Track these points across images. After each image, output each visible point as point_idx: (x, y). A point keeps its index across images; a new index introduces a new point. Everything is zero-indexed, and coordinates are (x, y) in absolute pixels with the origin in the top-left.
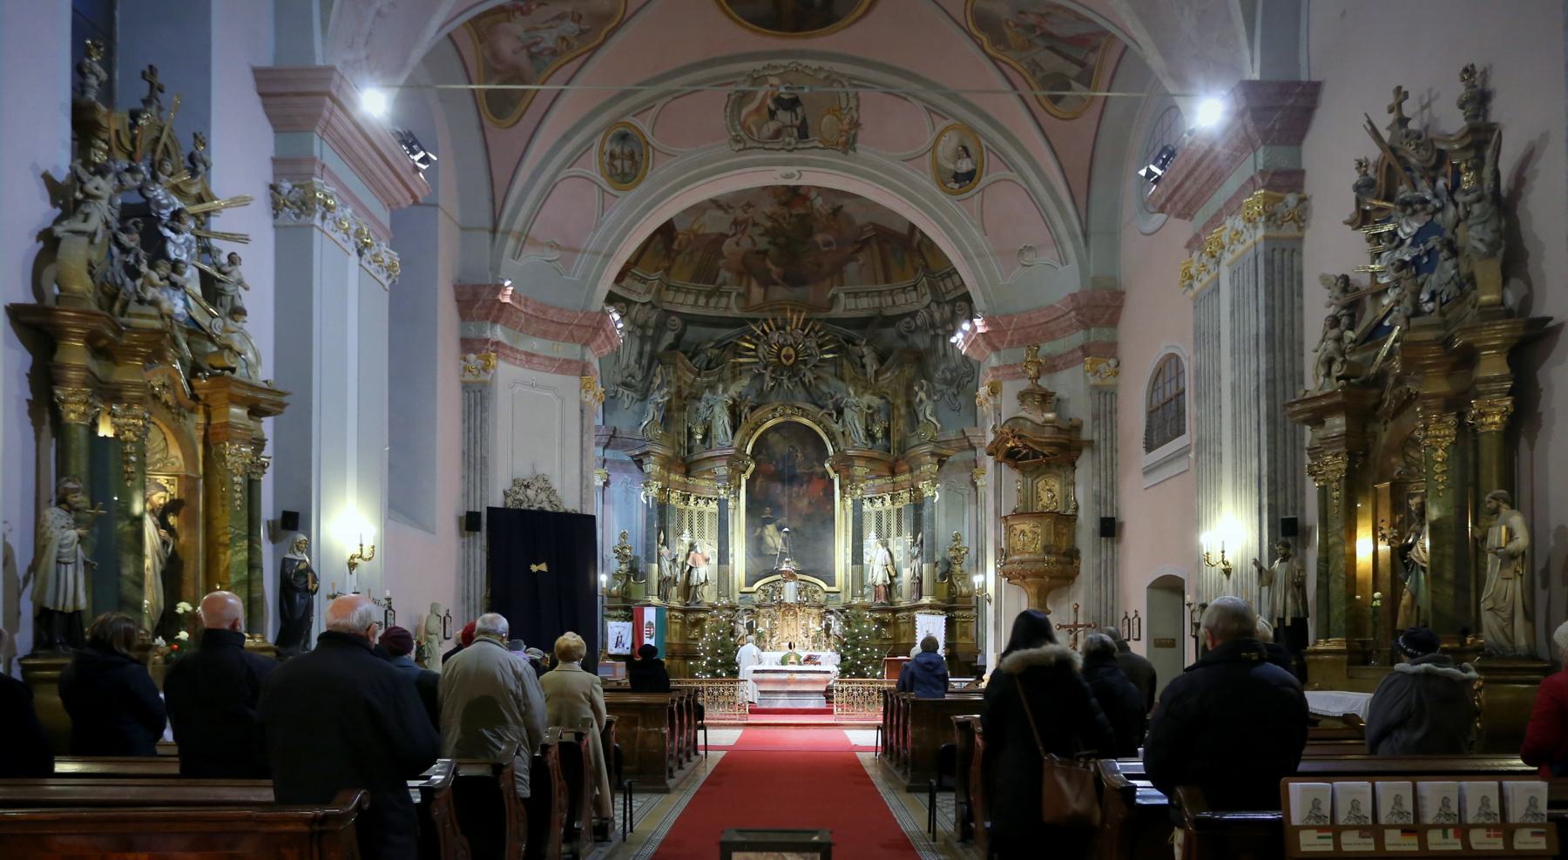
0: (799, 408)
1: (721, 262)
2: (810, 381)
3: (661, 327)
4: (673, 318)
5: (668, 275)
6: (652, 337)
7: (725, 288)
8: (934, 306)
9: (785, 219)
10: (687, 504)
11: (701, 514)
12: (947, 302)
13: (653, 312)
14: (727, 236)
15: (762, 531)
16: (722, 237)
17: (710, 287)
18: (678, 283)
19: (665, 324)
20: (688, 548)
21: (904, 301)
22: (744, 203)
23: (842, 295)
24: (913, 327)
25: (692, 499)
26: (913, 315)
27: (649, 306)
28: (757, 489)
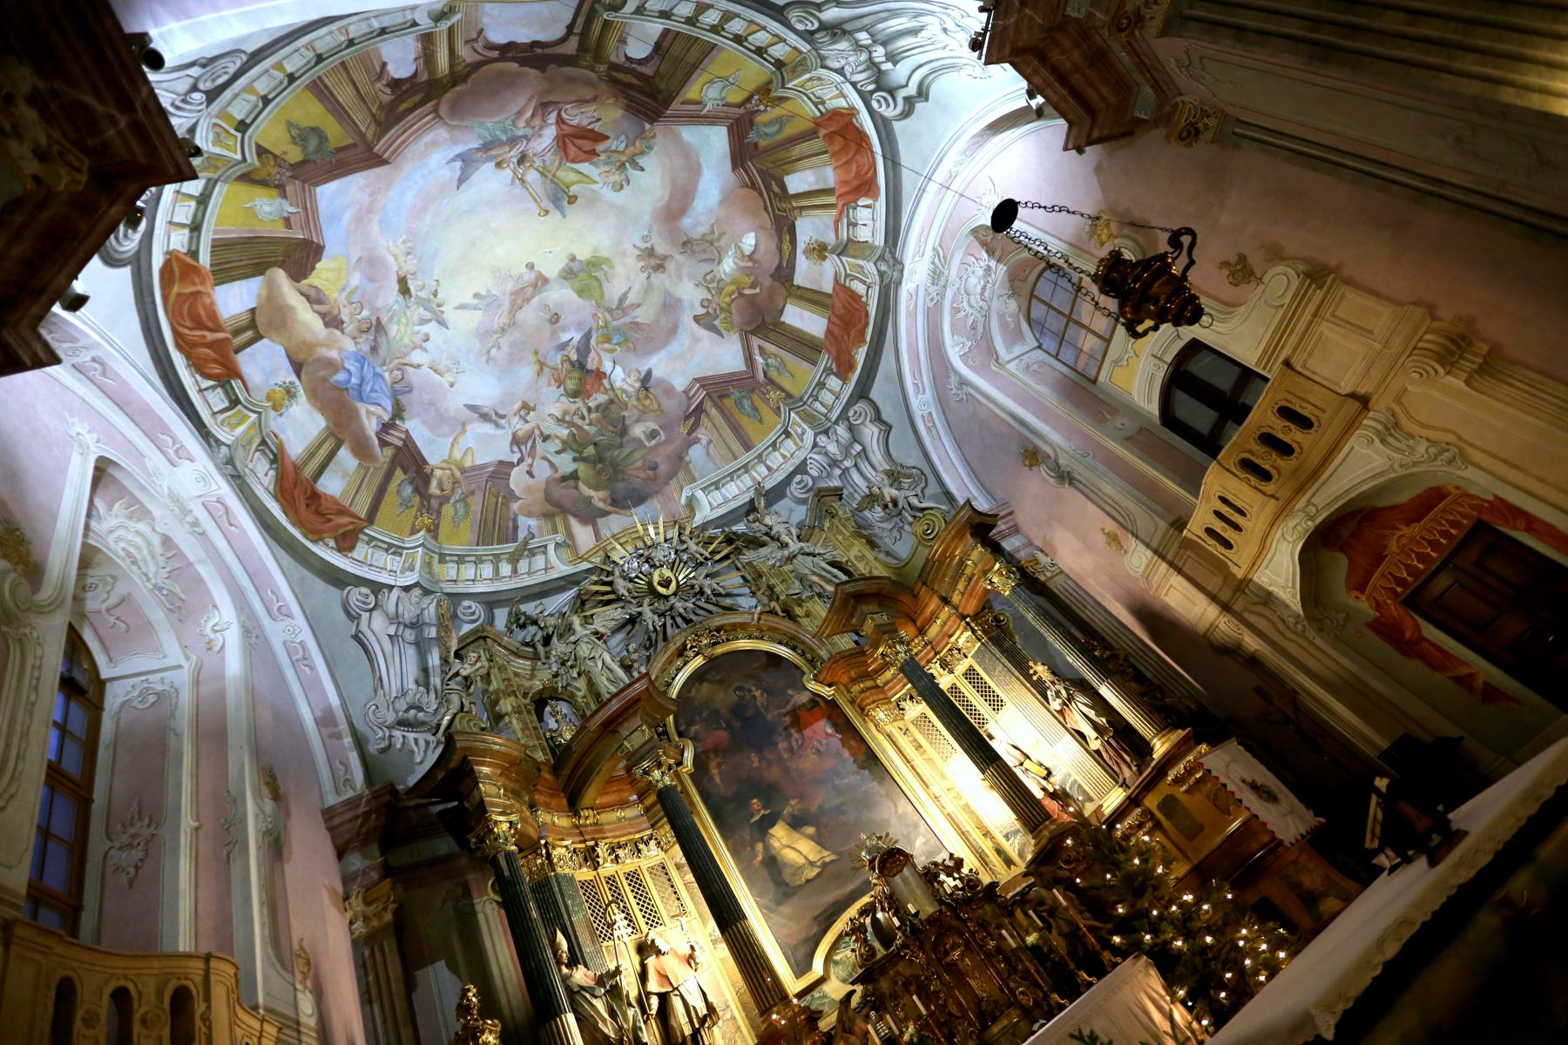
0: (718, 630)
1: (515, 506)
3: (448, 620)
4: (466, 603)
5: (436, 538)
6: (438, 639)
7: (534, 543)
8: (822, 440)
9: (583, 418)
10: (596, 866)
11: (634, 878)
12: (836, 422)
13: (427, 600)
14: (511, 465)
15: (767, 847)
16: (504, 468)
17: (510, 547)
18: (458, 548)
19: (454, 616)
21: (782, 461)
22: (518, 405)
23: (699, 494)
24: (810, 483)
25: (602, 850)
26: (801, 468)
27: (417, 592)
28: (717, 779)
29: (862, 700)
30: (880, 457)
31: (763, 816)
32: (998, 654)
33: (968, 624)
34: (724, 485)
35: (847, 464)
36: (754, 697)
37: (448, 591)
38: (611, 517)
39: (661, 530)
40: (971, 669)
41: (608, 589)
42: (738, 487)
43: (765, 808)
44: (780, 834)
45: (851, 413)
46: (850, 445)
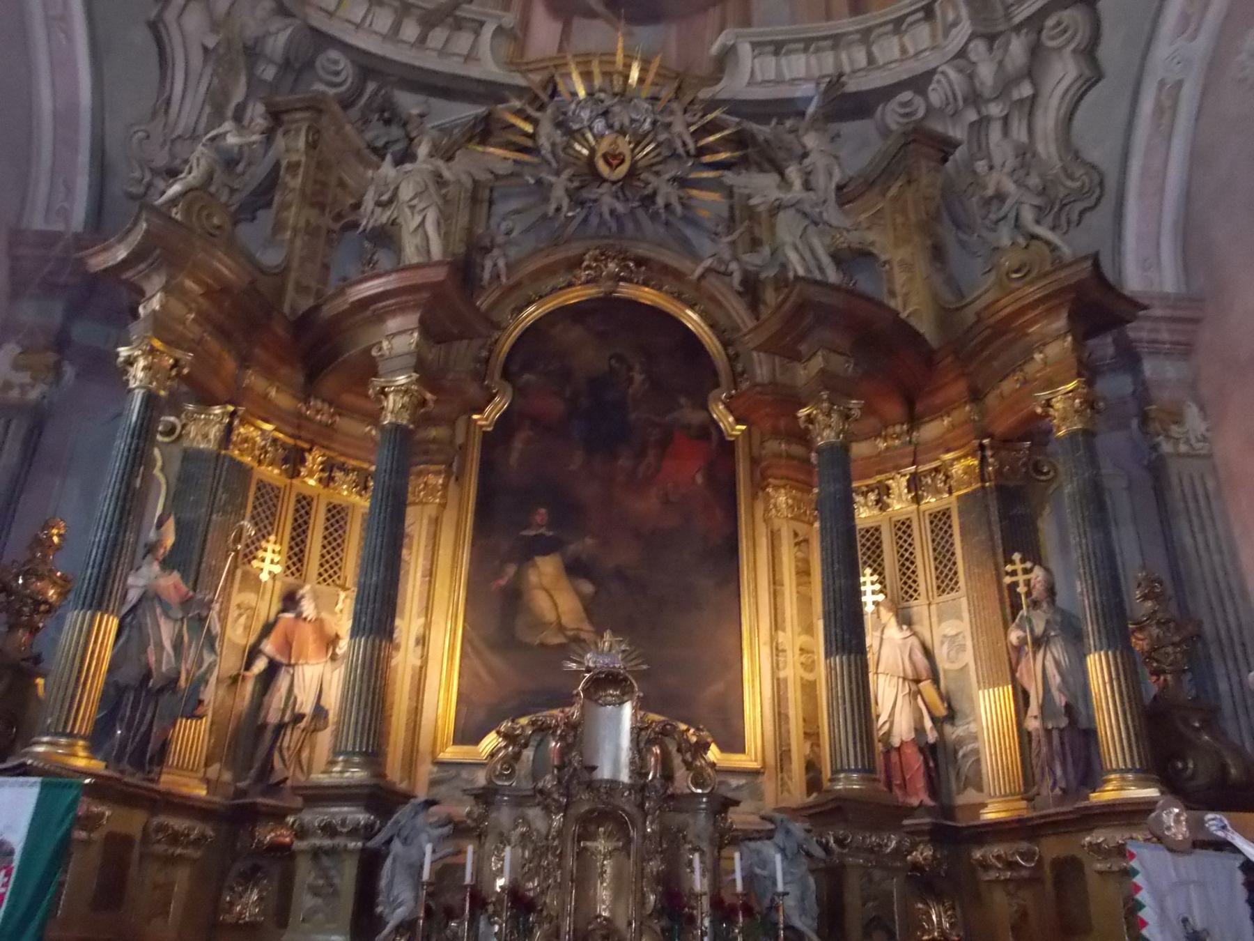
0: (640, 262)
2: (667, 206)
4: (333, 54)
8: (978, 48)
10: (295, 474)
11: (337, 514)
12: (1018, 28)
13: (276, 23)
15: (519, 575)
19: (309, 65)
20: (276, 606)
21: (896, 53)
23: (745, 49)
24: (921, 113)
25: (315, 459)
26: (919, 83)
29: (768, 467)
30: (1051, 123)
31: (542, 535)
32: (995, 517)
33: (982, 447)
34: (789, 52)
35: (995, 110)
36: (630, 380)
37: (315, 23)
38: (598, 23)
39: (651, 77)
40: (946, 513)
41: (529, 128)
42: (808, 65)
43: (549, 526)
44: (547, 568)
45: (1050, 22)
46: (1015, 81)
